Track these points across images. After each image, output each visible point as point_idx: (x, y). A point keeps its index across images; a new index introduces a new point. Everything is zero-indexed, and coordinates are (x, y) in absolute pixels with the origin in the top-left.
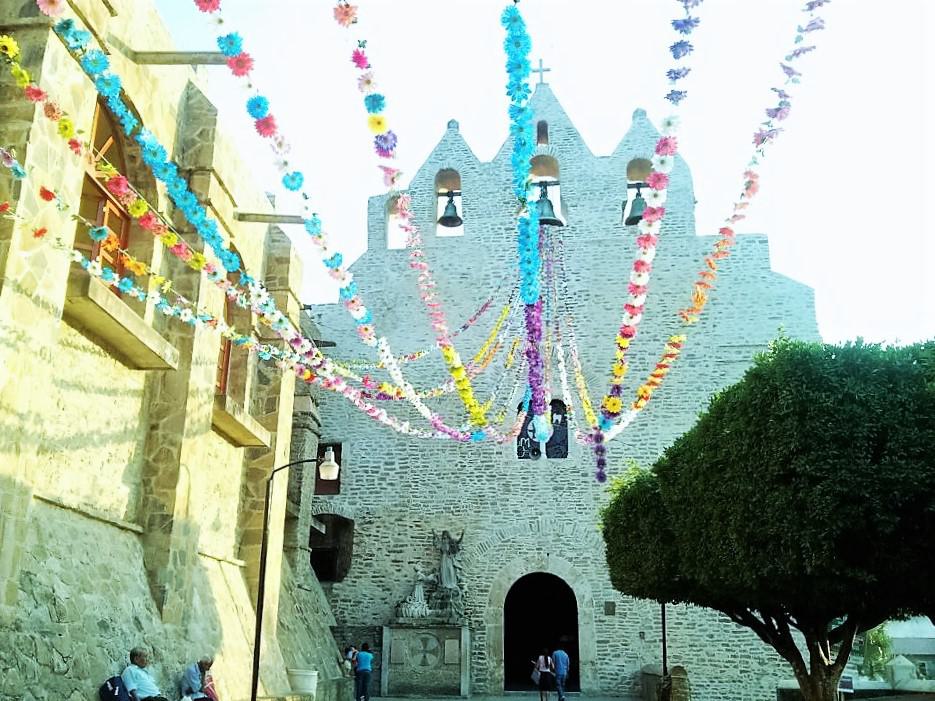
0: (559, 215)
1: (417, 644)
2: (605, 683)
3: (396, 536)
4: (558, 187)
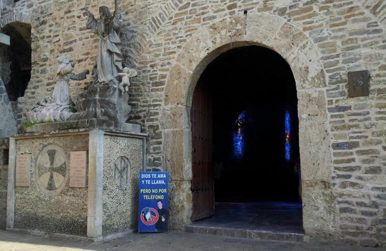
1: (44, 160)
2: (352, 220)
3: (66, 32)
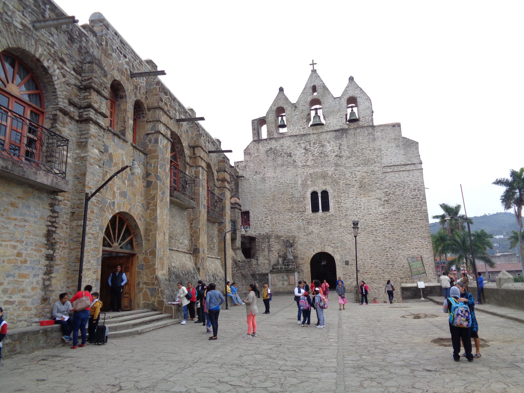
0: (323, 121)
4: (321, 110)
